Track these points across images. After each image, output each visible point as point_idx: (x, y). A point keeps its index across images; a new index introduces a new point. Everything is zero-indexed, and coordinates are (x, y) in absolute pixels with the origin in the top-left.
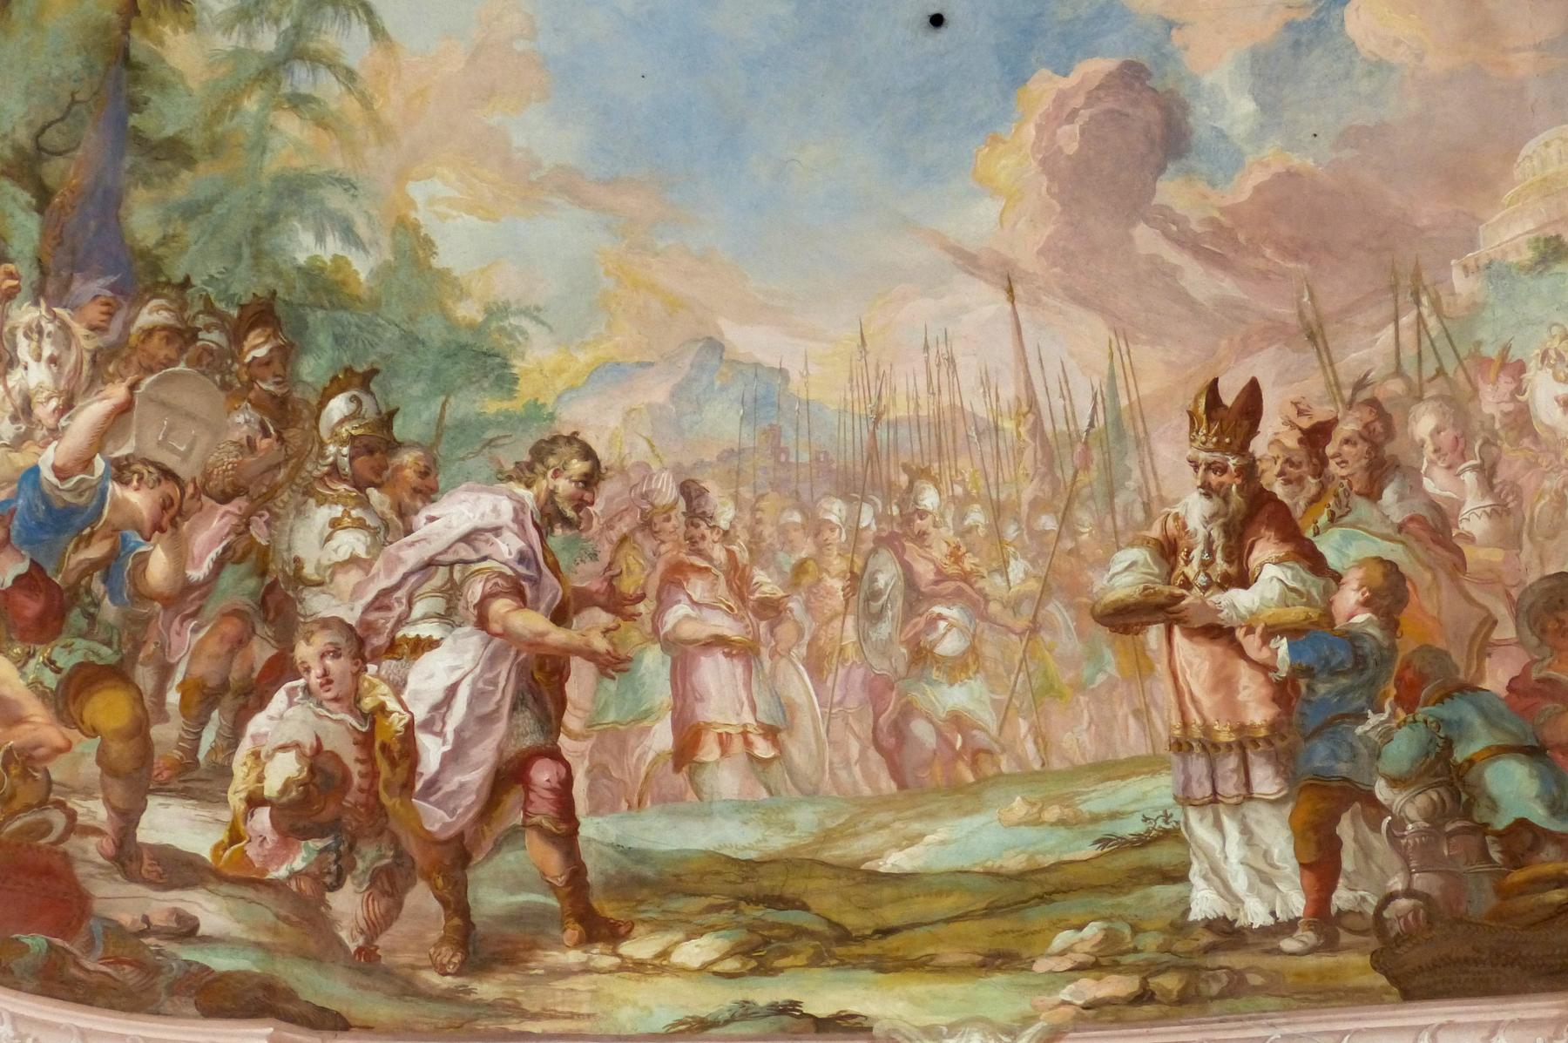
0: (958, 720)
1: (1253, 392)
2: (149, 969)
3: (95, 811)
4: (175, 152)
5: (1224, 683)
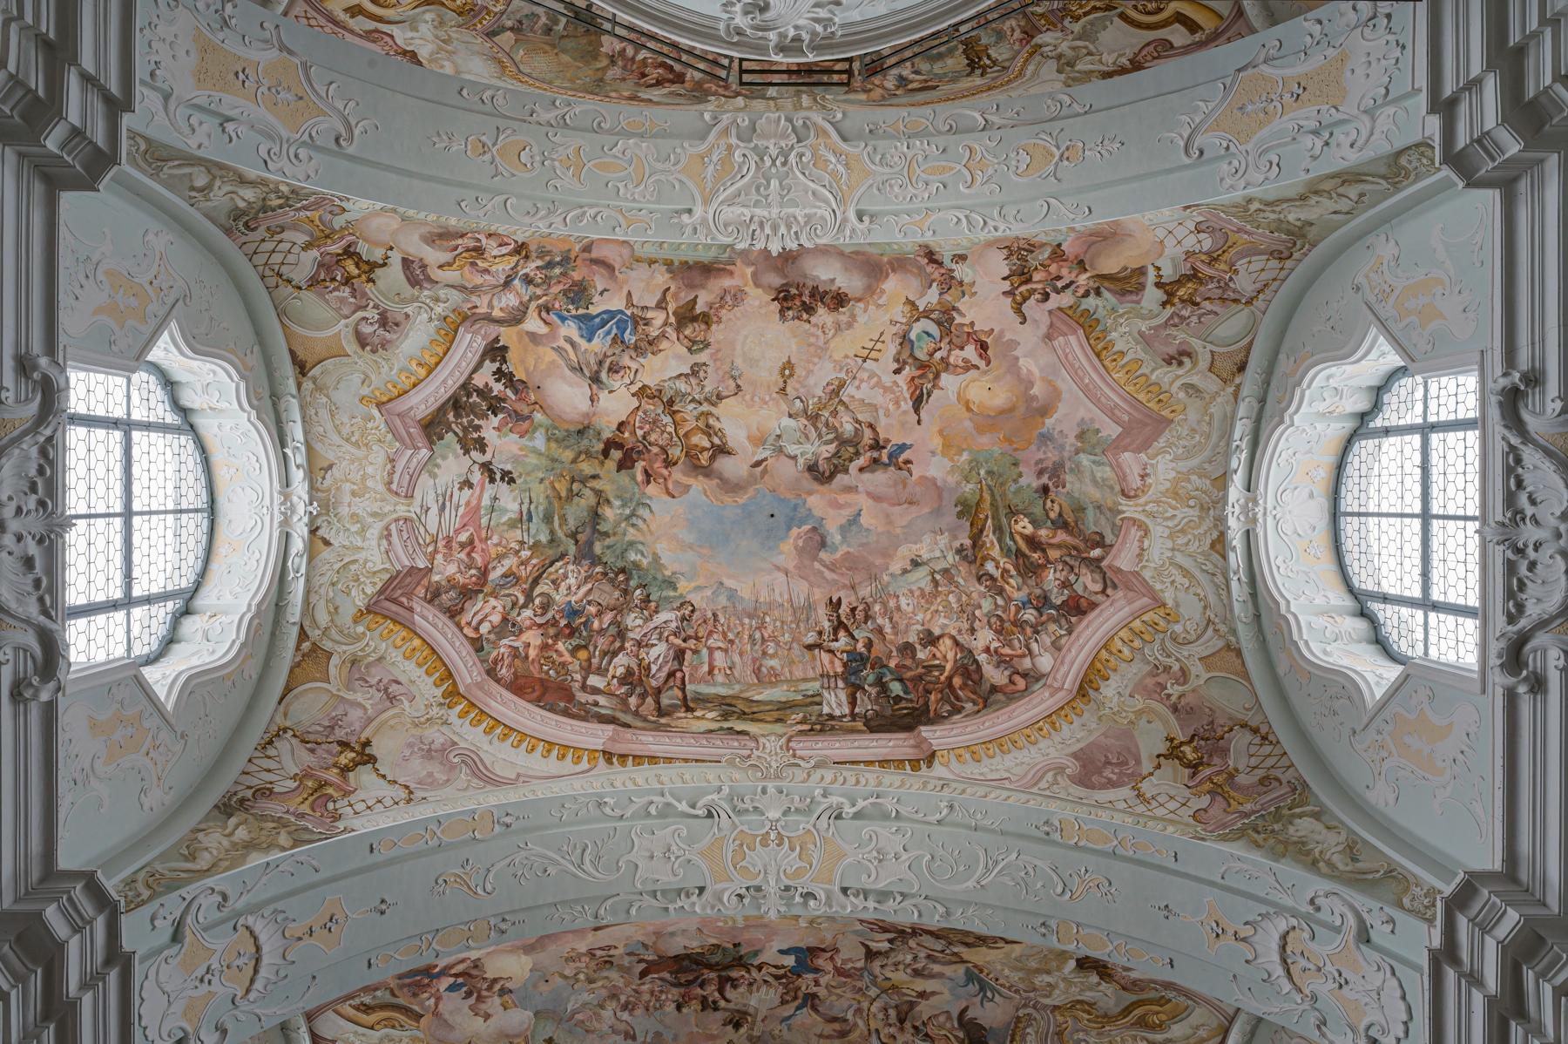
0: (772, 668)
1: (840, 599)
2: (587, 712)
3: (578, 677)
4: (606, 534)
5: (832, 662)
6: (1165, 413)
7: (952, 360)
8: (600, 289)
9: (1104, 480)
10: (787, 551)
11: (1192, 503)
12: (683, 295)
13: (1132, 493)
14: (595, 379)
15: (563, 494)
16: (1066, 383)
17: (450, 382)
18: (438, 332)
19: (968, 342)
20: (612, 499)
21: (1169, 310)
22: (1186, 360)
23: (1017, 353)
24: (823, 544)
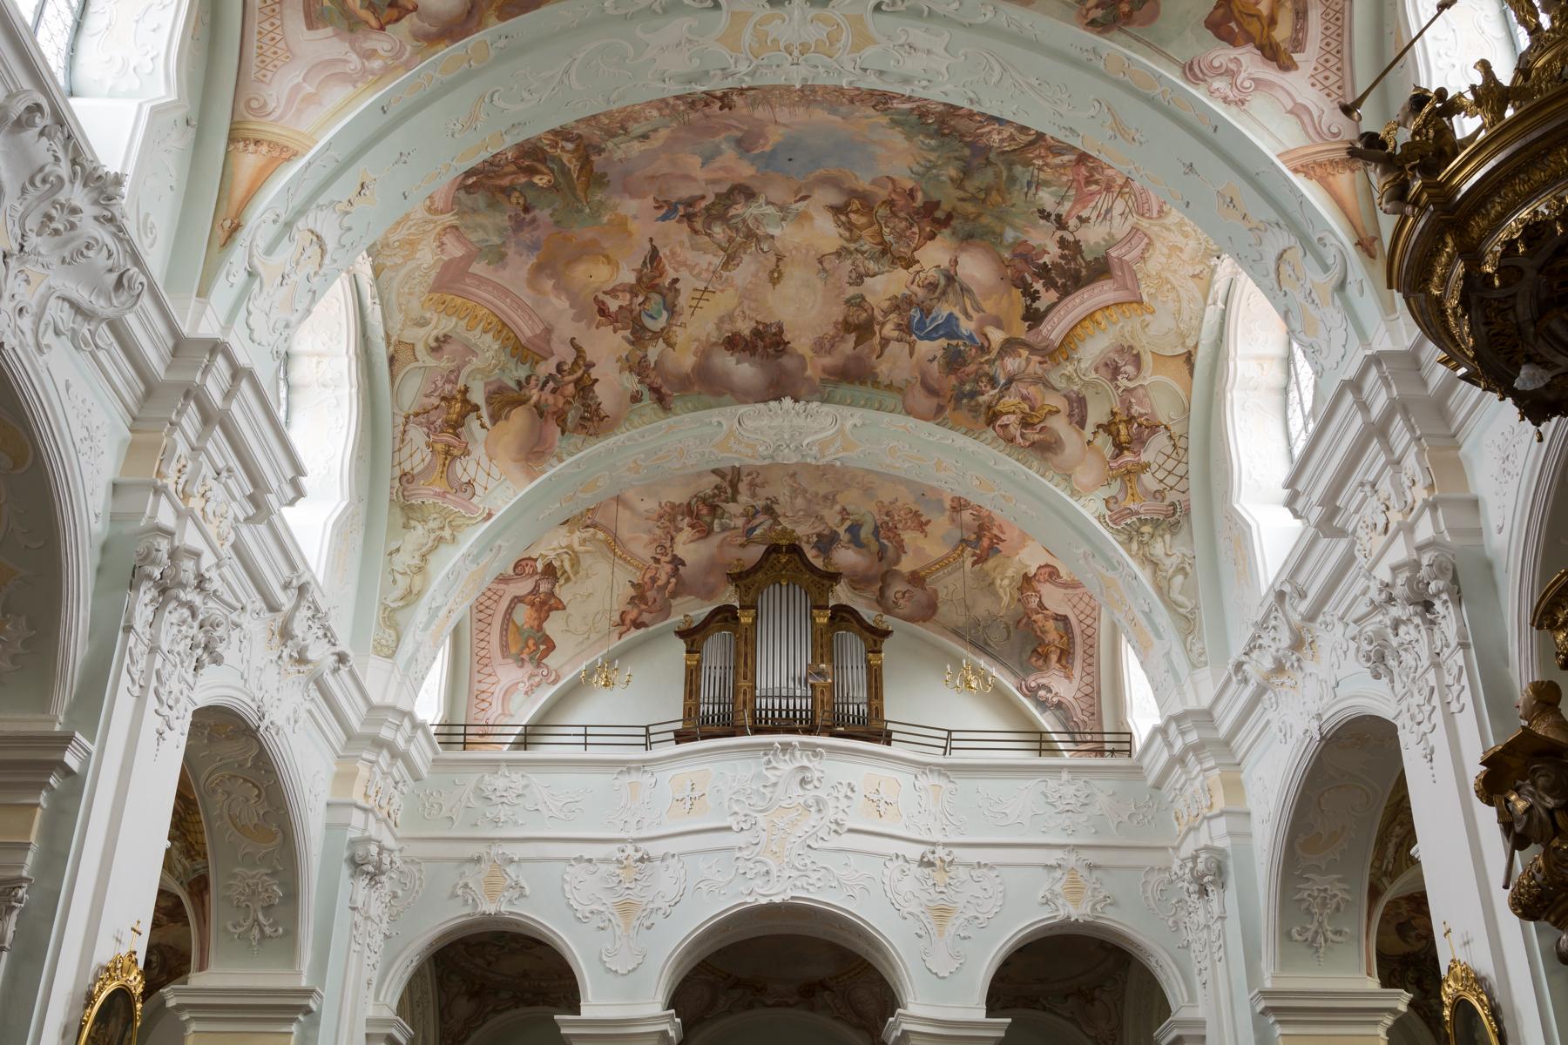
4: (957, 159)
6: (436, 296)
7: (628, 296)
8: (935, 363)
9: (476, 231)
10: (775, 136)
11: (397, 244)
12: (867, 351)
13: (448, 230)
14: (951, 279)
15: (994, 193)
16: (526, 295)
17: (1077, 301)
18: (1076, 346)
19: (617, 313)
20: (949, 181)
21: (461, 385)
22: (434, 344)
23: (573, 311)
24: (739, 142)
